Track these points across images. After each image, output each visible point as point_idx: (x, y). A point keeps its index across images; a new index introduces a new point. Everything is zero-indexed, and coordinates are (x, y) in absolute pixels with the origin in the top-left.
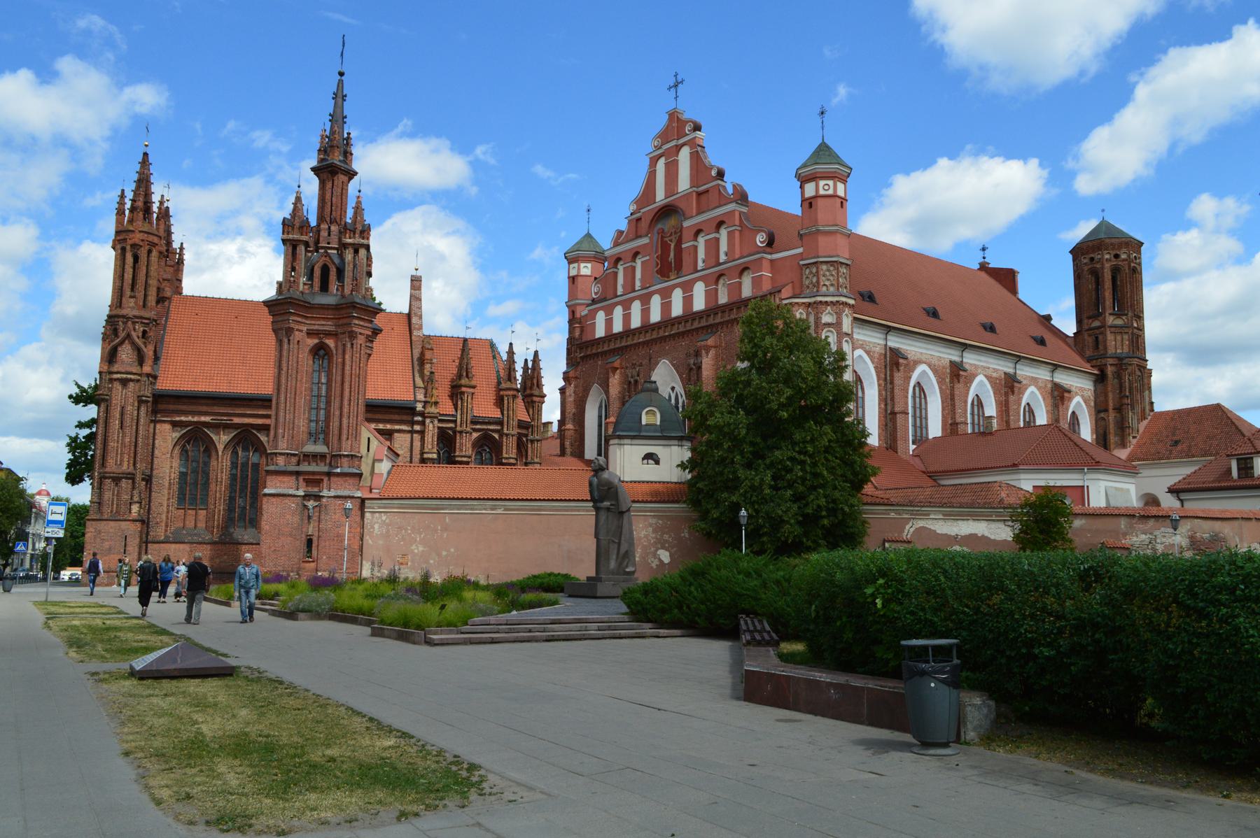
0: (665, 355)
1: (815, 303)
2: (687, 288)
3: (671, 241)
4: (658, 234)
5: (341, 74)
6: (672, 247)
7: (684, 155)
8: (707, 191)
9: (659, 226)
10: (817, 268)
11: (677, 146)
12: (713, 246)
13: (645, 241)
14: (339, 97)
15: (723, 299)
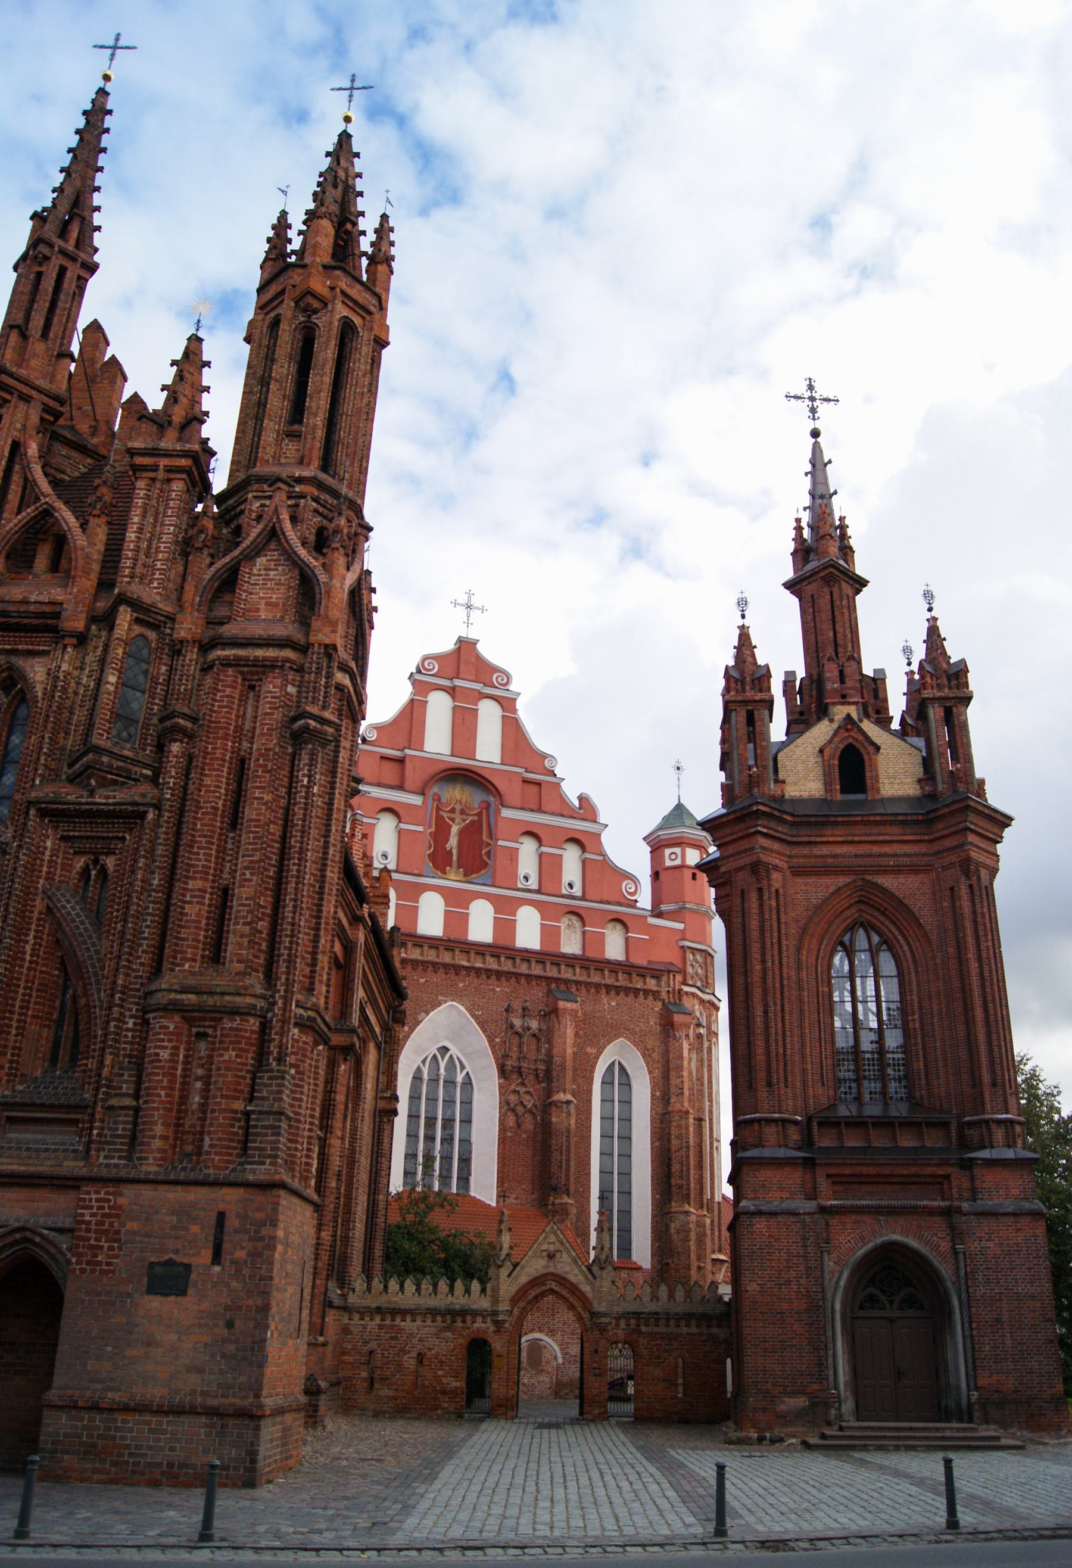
0: (458, 996)
1: (708, 1002)
2: (505, 908)
3: (453, 820)
4: (434, 800)
5: (815, 434)
6: (455, 829)
7: (489, 715)
8: (539, 784)
9: (435, 789)
10: (706, 958)
11: (480, 693)
12: (550, 867)
13: (417, 800)
14: (818, 465)
15: (571, 944)
